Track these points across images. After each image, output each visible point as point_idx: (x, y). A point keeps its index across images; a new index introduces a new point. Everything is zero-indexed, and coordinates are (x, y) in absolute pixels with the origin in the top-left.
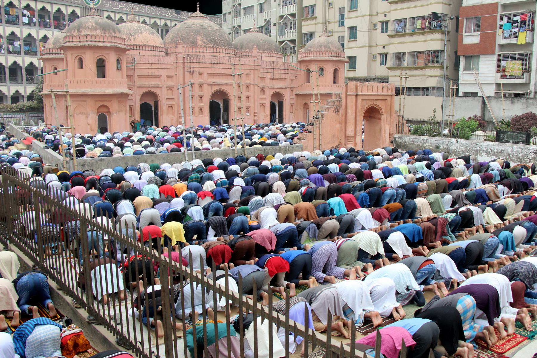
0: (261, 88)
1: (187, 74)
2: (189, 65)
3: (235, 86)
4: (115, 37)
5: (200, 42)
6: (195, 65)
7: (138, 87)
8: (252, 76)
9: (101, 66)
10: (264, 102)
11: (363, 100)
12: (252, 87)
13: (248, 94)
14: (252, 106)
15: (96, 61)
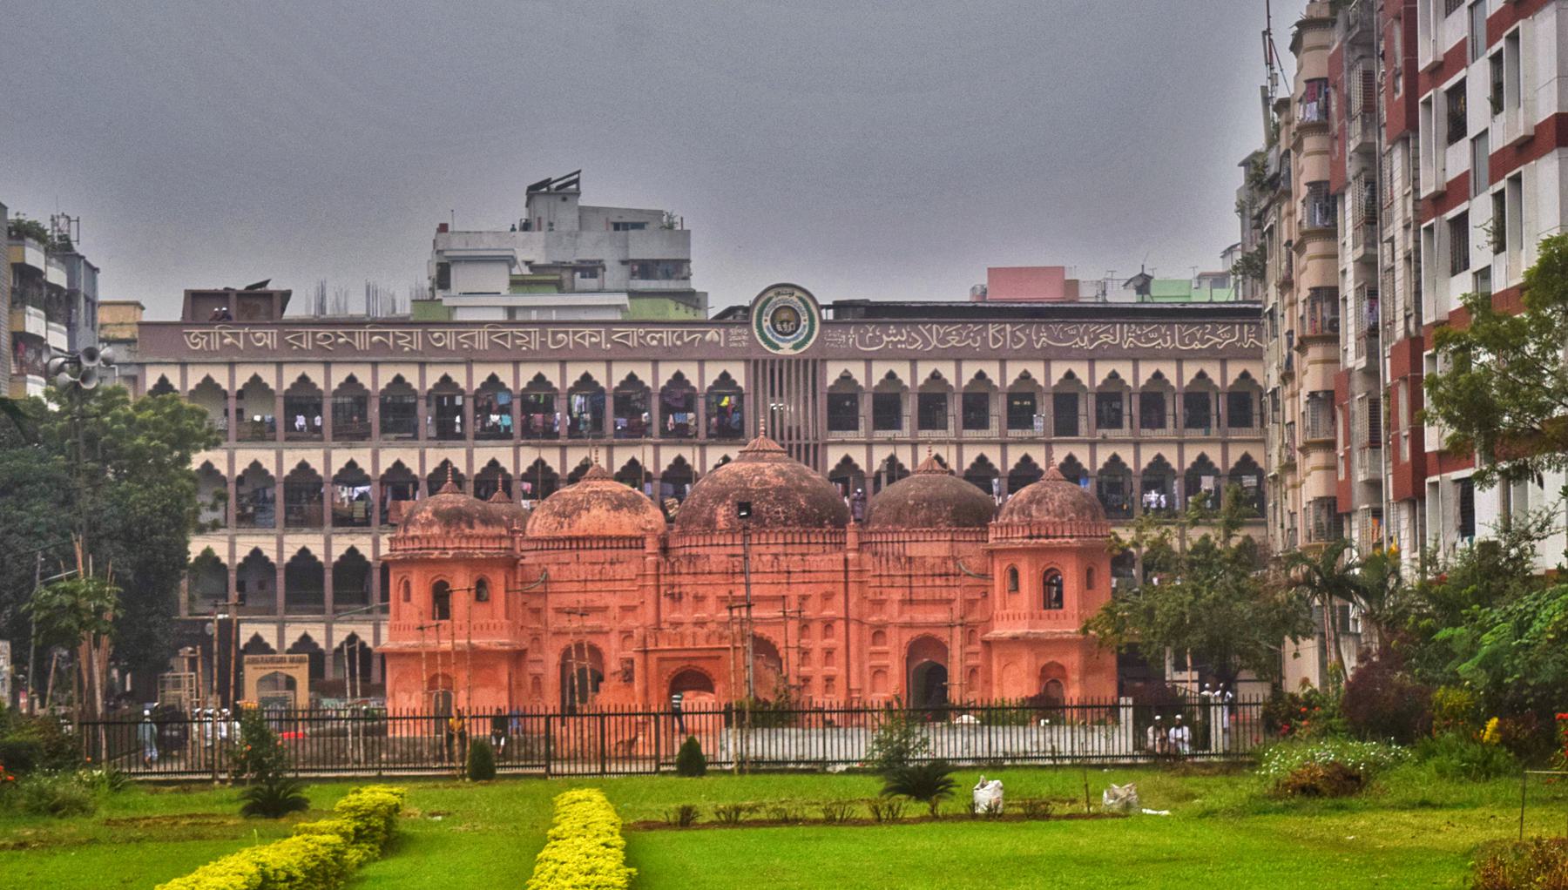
0: (872, 626)
1: (665, 602)
2: (669, 579)
3: (793, 626)
4: (469, 538)
5: (721, 522)
6: (686, 580)
7: (555, 634)
8: (842, 599)
9: (441, 598)
10: (885, 662)
11: (661, 660)
12: (840, 627)
13: (829, 642)
14: (842, 672)
15: (429, 587)
